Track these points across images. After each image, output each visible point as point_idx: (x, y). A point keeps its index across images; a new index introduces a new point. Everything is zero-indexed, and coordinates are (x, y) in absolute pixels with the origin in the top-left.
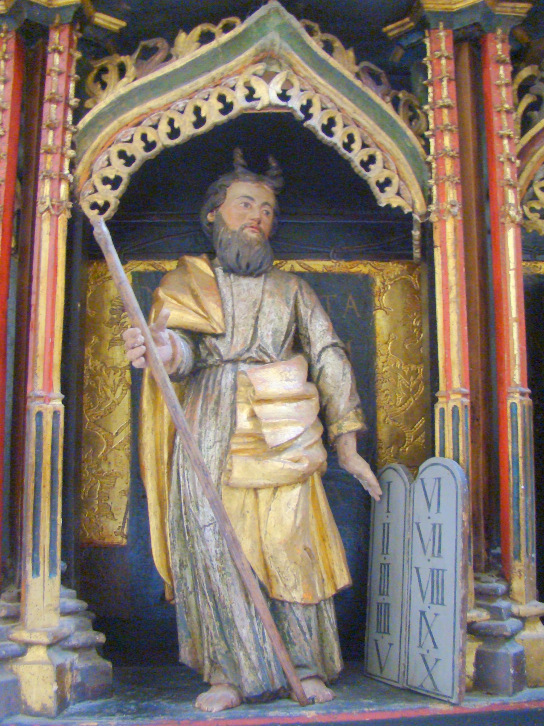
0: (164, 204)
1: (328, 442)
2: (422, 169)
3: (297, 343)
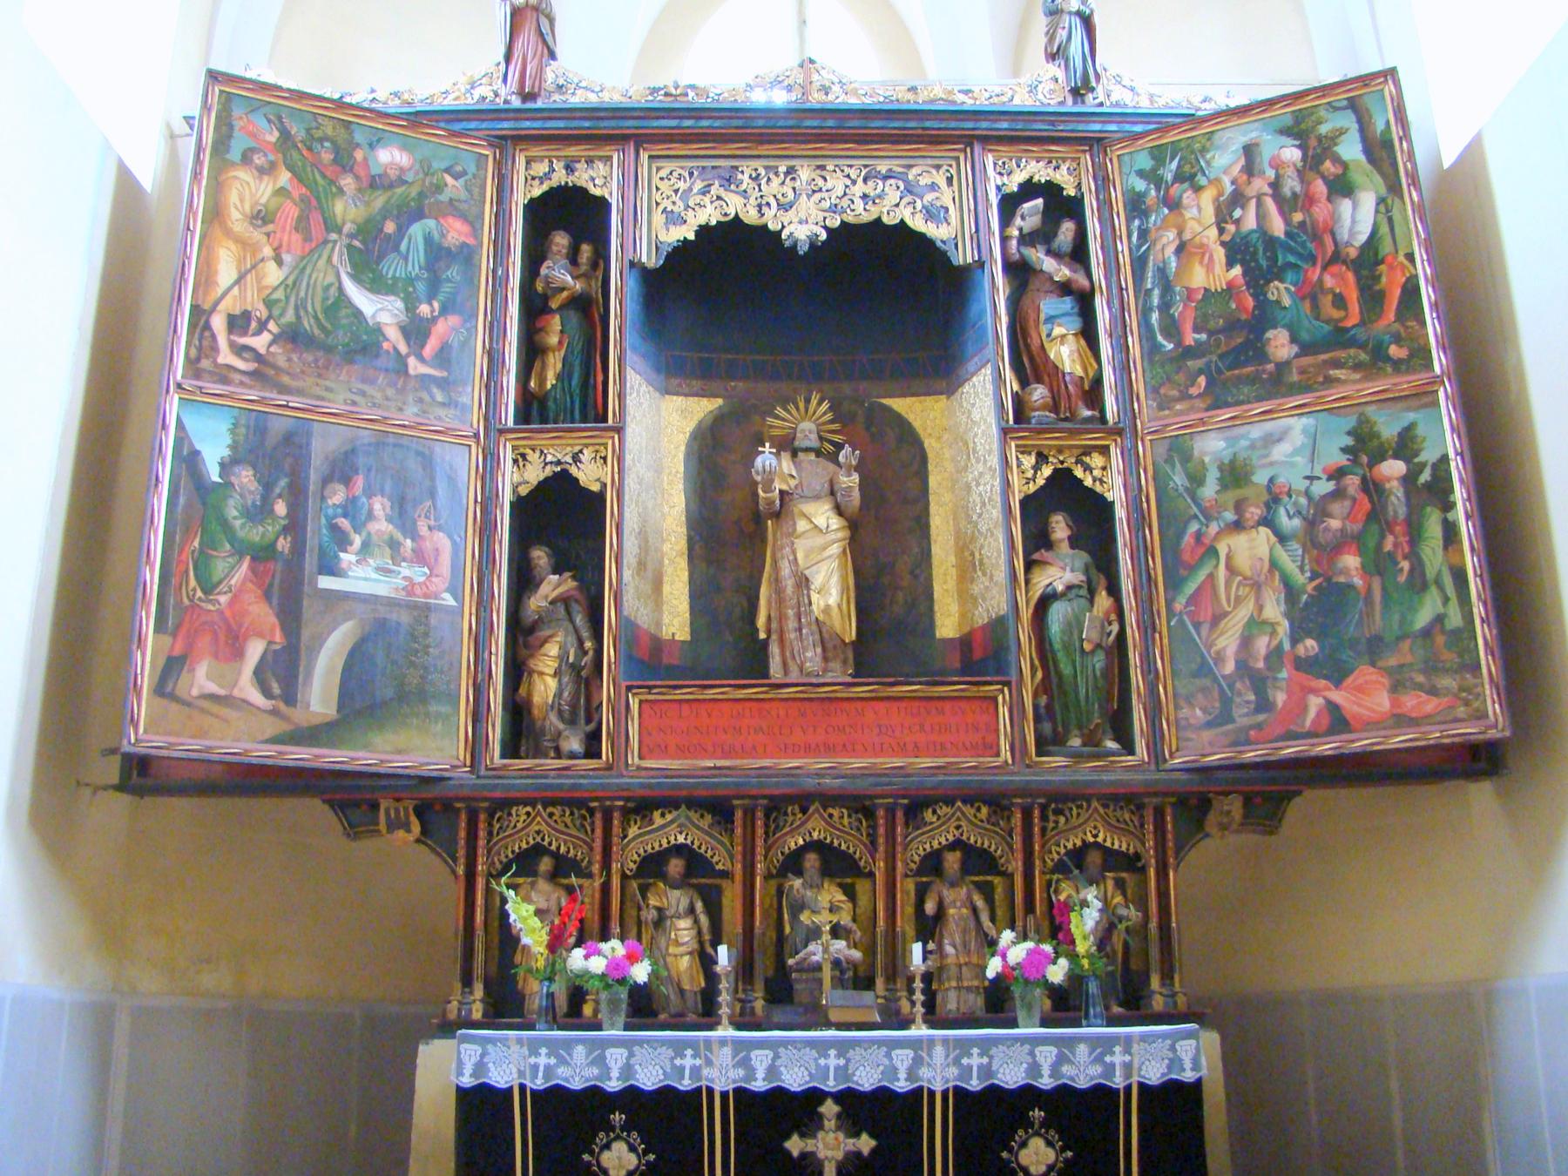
0: (652, 866)
1: (701, 943)
2: (732, 857)
3: (691, 910)
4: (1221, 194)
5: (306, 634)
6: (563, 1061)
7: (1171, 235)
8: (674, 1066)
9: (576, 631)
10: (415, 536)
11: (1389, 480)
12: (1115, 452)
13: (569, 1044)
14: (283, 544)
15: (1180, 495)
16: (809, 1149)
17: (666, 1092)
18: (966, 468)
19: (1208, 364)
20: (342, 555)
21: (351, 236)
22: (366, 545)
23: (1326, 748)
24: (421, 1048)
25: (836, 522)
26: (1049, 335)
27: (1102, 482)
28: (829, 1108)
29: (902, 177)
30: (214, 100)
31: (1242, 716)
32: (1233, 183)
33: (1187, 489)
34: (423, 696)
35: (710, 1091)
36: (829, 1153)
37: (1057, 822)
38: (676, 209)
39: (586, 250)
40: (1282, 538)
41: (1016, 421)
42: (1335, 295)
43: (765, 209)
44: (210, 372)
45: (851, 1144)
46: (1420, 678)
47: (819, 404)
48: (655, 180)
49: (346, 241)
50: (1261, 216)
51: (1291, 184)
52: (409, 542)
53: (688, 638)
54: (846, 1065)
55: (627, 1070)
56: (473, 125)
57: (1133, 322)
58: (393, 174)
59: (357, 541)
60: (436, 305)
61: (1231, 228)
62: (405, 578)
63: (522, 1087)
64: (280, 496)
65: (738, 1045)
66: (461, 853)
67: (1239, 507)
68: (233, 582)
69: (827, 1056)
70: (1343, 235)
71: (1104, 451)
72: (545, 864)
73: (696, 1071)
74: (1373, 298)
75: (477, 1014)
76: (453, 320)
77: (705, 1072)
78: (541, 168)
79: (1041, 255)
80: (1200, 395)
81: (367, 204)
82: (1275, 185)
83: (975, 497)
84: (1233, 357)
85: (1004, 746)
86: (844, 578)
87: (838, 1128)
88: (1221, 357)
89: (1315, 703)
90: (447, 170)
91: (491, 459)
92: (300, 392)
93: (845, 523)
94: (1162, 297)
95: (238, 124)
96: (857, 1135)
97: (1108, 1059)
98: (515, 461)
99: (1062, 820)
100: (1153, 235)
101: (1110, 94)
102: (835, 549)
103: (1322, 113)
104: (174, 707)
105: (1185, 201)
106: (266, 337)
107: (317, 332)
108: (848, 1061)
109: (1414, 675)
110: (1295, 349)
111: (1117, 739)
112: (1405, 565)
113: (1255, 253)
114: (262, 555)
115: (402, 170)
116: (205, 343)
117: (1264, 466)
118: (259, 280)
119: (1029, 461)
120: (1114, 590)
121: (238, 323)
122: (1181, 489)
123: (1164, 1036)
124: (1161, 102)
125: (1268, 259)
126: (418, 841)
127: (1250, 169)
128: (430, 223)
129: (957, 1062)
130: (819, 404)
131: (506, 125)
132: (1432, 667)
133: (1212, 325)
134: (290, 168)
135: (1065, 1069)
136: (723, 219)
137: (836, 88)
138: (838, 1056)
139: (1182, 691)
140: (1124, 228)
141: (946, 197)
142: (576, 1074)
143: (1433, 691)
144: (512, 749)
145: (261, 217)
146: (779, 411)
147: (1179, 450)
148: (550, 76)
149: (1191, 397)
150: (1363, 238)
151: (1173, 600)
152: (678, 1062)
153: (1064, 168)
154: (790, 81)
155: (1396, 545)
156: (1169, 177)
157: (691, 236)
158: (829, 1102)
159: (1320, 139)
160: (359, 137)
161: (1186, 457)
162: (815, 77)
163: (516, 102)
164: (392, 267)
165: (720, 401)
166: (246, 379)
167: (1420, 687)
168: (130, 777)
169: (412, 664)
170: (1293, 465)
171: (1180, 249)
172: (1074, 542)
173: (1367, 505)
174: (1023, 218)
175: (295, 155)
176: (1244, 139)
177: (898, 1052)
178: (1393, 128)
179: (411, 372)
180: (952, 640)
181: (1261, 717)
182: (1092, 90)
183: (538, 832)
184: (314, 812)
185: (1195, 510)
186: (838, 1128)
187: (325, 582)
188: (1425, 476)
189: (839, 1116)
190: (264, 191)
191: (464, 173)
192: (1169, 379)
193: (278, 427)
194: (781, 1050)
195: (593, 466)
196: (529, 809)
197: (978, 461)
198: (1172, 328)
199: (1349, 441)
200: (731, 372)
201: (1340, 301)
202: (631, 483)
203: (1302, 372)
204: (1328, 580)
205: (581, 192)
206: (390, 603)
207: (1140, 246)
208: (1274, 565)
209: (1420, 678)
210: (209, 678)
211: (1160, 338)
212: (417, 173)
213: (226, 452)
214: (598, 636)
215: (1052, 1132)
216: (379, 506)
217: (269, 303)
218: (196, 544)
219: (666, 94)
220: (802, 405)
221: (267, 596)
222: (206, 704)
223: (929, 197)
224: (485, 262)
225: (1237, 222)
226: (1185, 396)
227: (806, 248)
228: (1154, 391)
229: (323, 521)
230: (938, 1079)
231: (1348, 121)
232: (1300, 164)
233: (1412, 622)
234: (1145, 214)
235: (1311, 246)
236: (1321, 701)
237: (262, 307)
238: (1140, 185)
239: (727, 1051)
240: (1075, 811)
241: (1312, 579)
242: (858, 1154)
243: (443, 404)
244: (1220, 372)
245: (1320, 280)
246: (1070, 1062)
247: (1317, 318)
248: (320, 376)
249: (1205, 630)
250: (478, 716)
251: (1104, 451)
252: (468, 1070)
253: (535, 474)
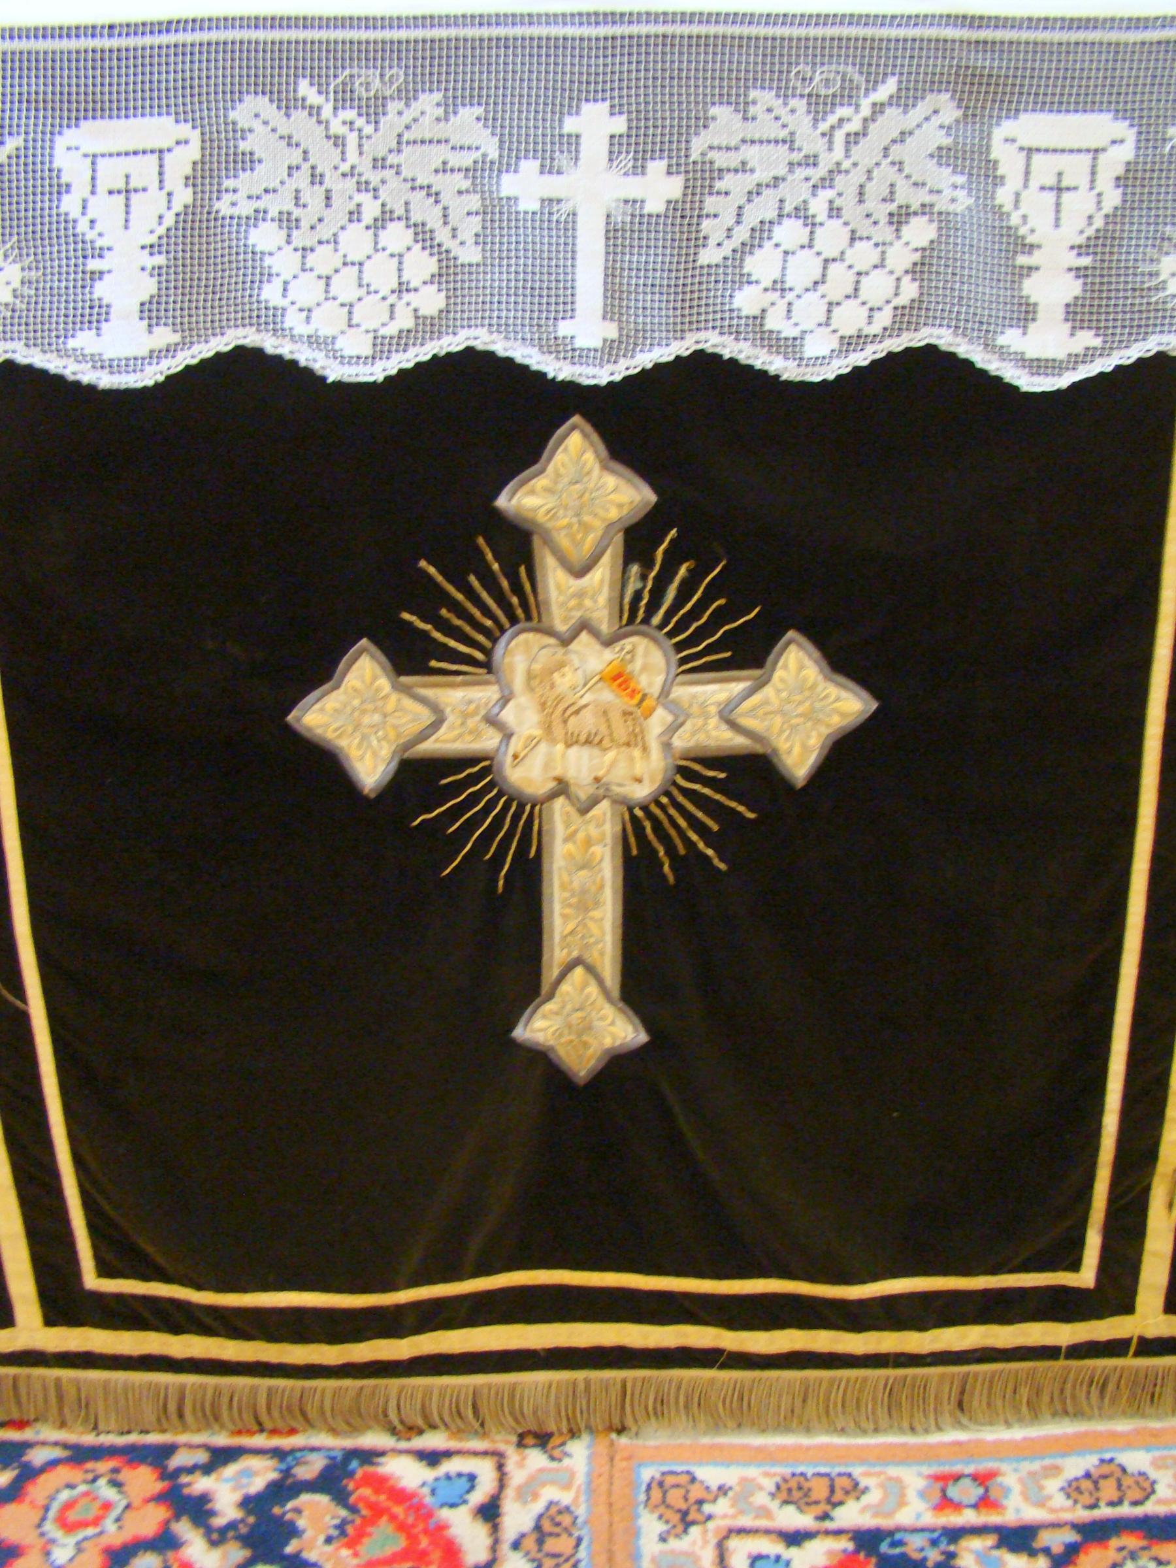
16: (447, 742)
28: (576, 494)
36: (580, 766)
45: (712, 711)
54: (685, 216)
87: (634, 615)
96: (749, 653)
108: (701, 179)
138: (632, 149)
158: (575, 450)
177: (1032, 127)
186: (634, 615)
189: (638, 540)
194: (252, 111)
242: (751, 771)
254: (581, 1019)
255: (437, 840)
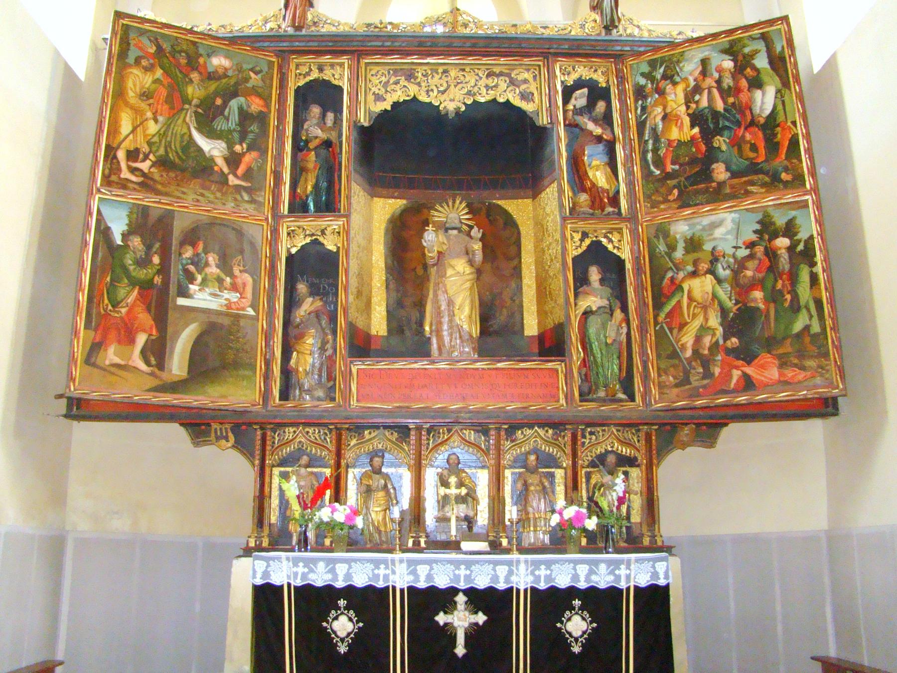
4: (688, 86)
5: (170, 330)
6: (312, 571)
7: (659, 109)
8: (374, 574)
9: (323, 329)
10: (233, 276)
11: (780, 248)
12: (626, 232)
13: (315, 561)
14: (158, 280)
15: (663, 256)
16: (449, 621)
17: (370, 588)
18: (542, 240)
19: (679, 183)
20: (191, 286)
21: (197, 106)
22: (204, 282)
23: (742, 399)
24: (235, 562)
25: (468, 270)
26: (589, 165)
27: (618, 248)
28: (461, 599)
29: (509, 75)
30: (119, 29)
31: (696, 380)
32: (695, 80)
33: (666, 253)
34: (236, 365)
35: (394, 588)
36: (461, 623)
37: (590, 439)
38: (380, 93)
39: (330, 116)
40: (719, 281)
41: (570, 214)
42: (751, 144)
43: (431, 93)
44: (117, 183)
46: (796, 361)
47: (461, 203)
48: (369, 76)
49: (194, 109)
50: (711, 99)
51: (728, 81)
52: (228, 280)
53: (386, 334)
55: (348, 576)
56: (266, 44)
57: (637, 157)
58: (221, 71)
59: (199, 278)
60: (245, 146)
61: (693, 106)
62: (226, 299)
63: (289, 585)
64: (156, 253)
65: (410, 562)
66: (258, 452)
67: (695, 263)
68: (129, 301)
69: (459, 569)
70: (757, 110)
71: (620, 231)
72: (305, 460)
73: (386, 577)
74: (773, 147)
75: (265, 544)
76: (254, 154)
77: (391, 577)
78: (305, 69)
79: (586, 120)
80: (674, 200)
81: (206, 88)
82: (719, 82)
83: (547, 257)
84: (691, 179)
85: (561, 396)
86: (472, 302)
87: (466, 609)
88: (686, 179)
89: (736, 374)
90: (252, 70)
91: (275, 232)
92: (167, 194)
93: (473, 270)
94: (654, 144)
95: (132, 42)
97: (617, 572)
98: (289, 234)
99: (594, 437)
100: (649, 110)
101: (625, 30)
102: (468, 285)
103: (746, 41)
104: (96, 370)
105: (668, 90)
106: (148, 163)
107: (177, 160)
108: (472, 571)
109: (792, 359)
110: (729, 174)
111: (624, 393)
112: (788, 297)
113: (707, 120)
114: (145, 286)
115: (226, 69)
116: (114, 166)
117: (710, 240)
118: (144, 131)
119: (577, 237)
120: (624, 309)
121: (133, 155)
122: (663, 253)
123: (649, 560)
124: (654, 34)
125: (714, 123)
126: (233, 447)
127: (704, 73)
128: (242, 99)
129: (532, 573)
130: (461, 203)
131: (285, 44)
132: (801, 355)
133: (681, 161)
134: (161, 68)
135: (594, 578)
136: (407, 98)
137: (472, 25)
138: (466, 569)
139: (663, 366)
140: (633, 105)
141: (533, 87)
142: (319, 578)
143: (803, 368)
144: (285, 395)
145: (146, 95)
146: (438, 207)
147: (662, 232)
148: (309, 17)
149: (669, 201)
150: (767, 112)
151: (658, 315)
152: (376, 572)
153: (599, 72)
154: (445, 20)
155: (783, 286)
156: (659, 77)
157: (389, 108)
158: (461, 595)
159: (744, 56)
160: (201, 51)
161: (666, 235)
162: (460, 18)
163: (291, 31)
164: (220, 124)
165: (404, 202)
166: (136, 187)
167: (796, 365)
168: (72, 410)
169: (231, 348)
170: (726, 240)
171: (665, 117)
172: (602, 281)
173: (767, 263)
174: (576, 99)
175: (165, 61)
176: (701, 56)
178: (786, 50)
179: (230, 183)
180: (533, 336)
181: (705, 382)
182: (616, 27)
183: (300, 442)
184: (175, 432)
185: (671, 264)
186: (466, 609)
187: (181, 301)
188: (801, 247)
190: (147, 80)
191: (261, 71)
192: (657, 191)
193: (154, 216)
194: (434, 565)
195: (332, 236)
196: (294, 429)
197: (549, 236)
198: (659, 162)
199: (758, 227)
200: (411, 184)
201: (754, 148)
202: (354, 247)
203: (732, 187)
204: (745, 304)
205: (326, 83)
206: (218, 313)
207: (641, 116)
208: (715, 296)
209: (796, 361)
210: (115, 354)
211: (652, 168)
212: (234, 71)
213: (126, 228)
214: (334, 332)
215: (585, 612)
216: (212, 259)
217: (150, 144)
218: (108, 279)
219: (376, 27)
220: (450, 204)
221: (149, 310)
222: (113, 369)
223: (523, 87)
224: (273, 121)
225: (697, 103)
226: (666, 201)
227: (453, 115)
228: (648, 197)
229: (180, 267)
230: (522, 581)
231: (761, 46)
232: (733, 70)
233: (791, 329)
234: (645, 98)
235: (738, 116)
236: (739, 373)
237: (146, 146)
238: (642, 81)
239: (404, 565)
240: (601, 434)
241: (736, 304)
242: (476, 624)
243: (248, 202)
244: (686, 187)
245: (743, 136)
246: (596, 573)
247: (741, 157)
248: (178, 185)
249: (675, 331)
250: (267, 377)
251: (620, 231)
252: (259, 575)
253: (301, 241)
254: (460, 650)
255: (448, 630)
